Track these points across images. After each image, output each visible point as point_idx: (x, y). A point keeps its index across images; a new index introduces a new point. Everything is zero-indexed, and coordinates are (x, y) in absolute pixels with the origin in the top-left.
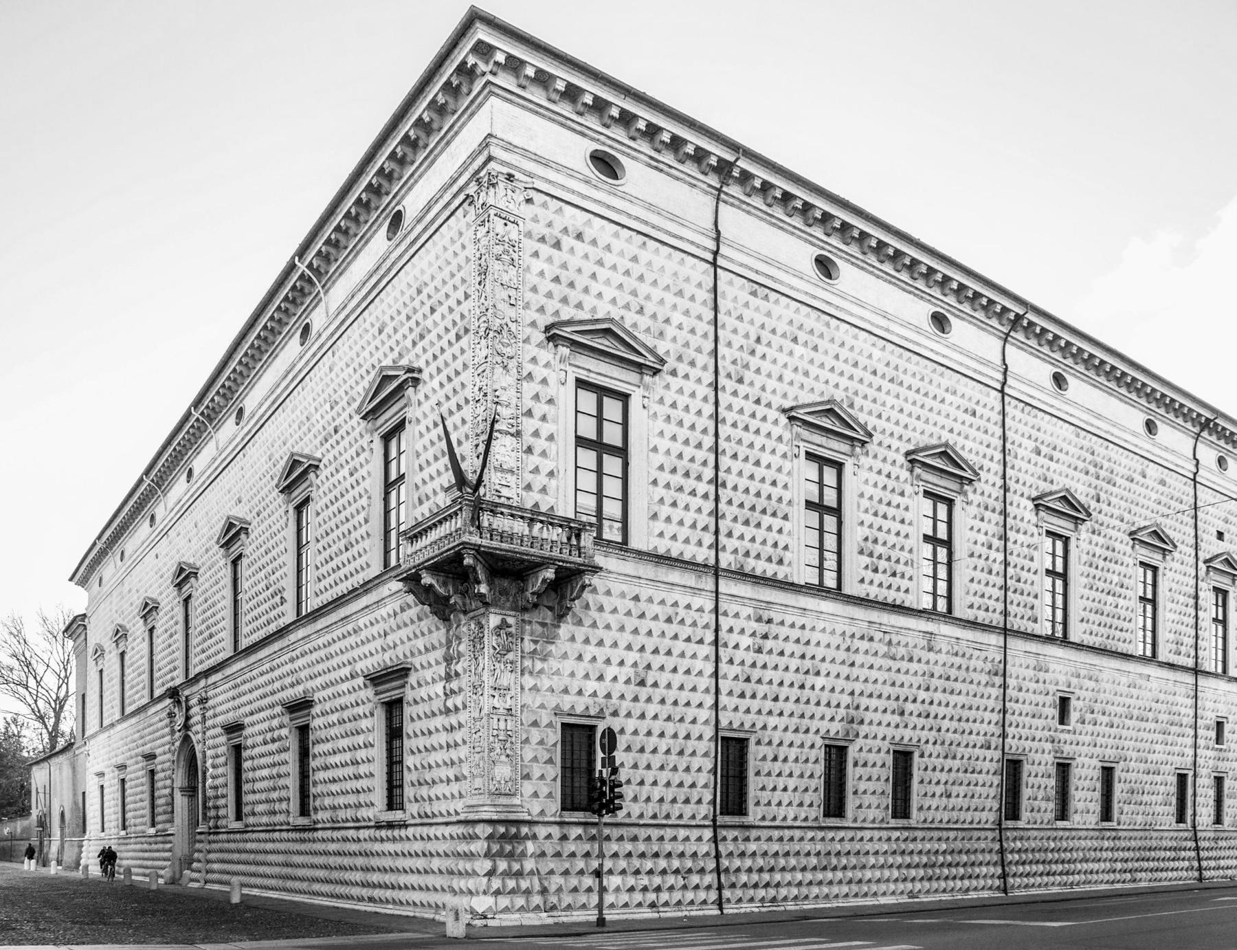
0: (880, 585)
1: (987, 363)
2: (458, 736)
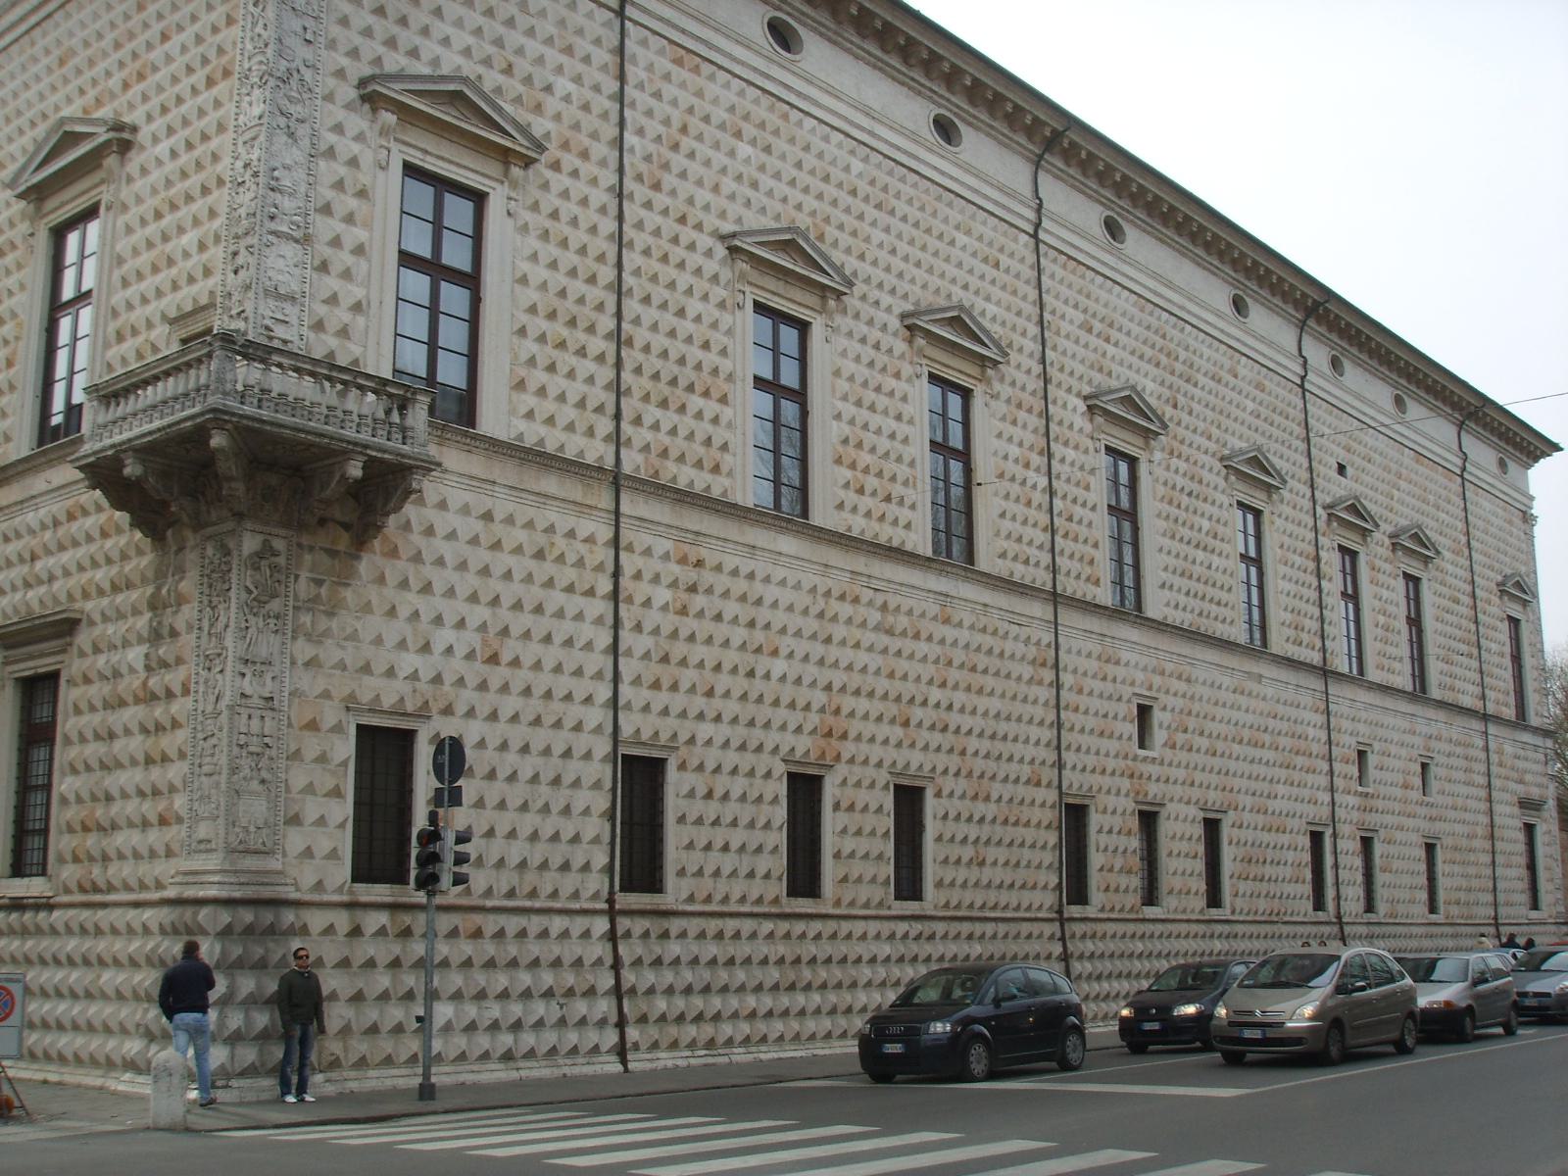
0: (868, 514)
1: (1011, 194)
2: (170, 742)
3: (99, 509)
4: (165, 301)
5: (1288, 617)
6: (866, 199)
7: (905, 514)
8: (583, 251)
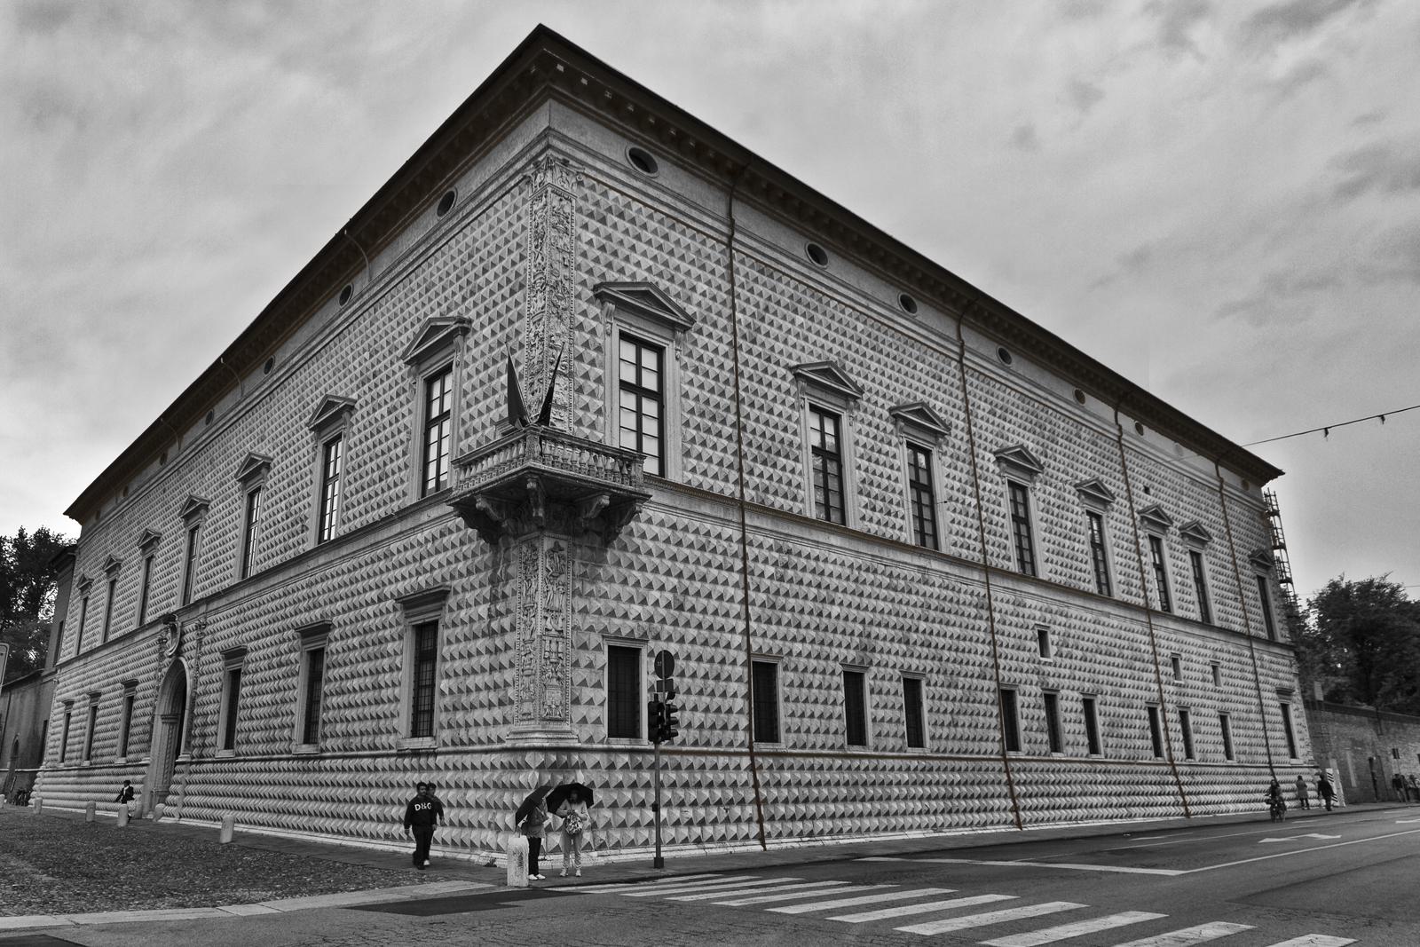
2: (504, 658)
3: (459, 529)
4: (491, 414)
5: (1122, 578)
7: (899, 522)
8: (716, 378)
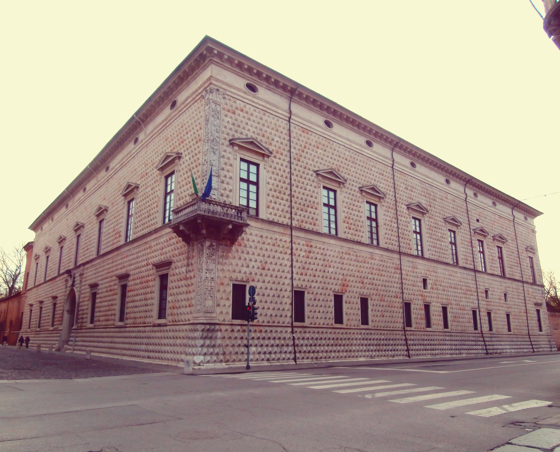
2: (191, 288)
3: (176, 237)
6: (350, 161)
